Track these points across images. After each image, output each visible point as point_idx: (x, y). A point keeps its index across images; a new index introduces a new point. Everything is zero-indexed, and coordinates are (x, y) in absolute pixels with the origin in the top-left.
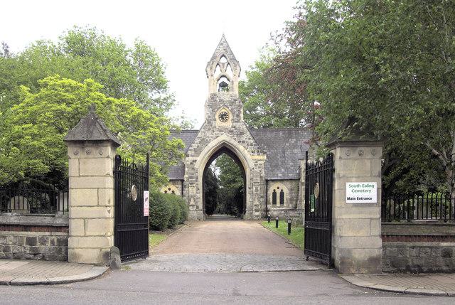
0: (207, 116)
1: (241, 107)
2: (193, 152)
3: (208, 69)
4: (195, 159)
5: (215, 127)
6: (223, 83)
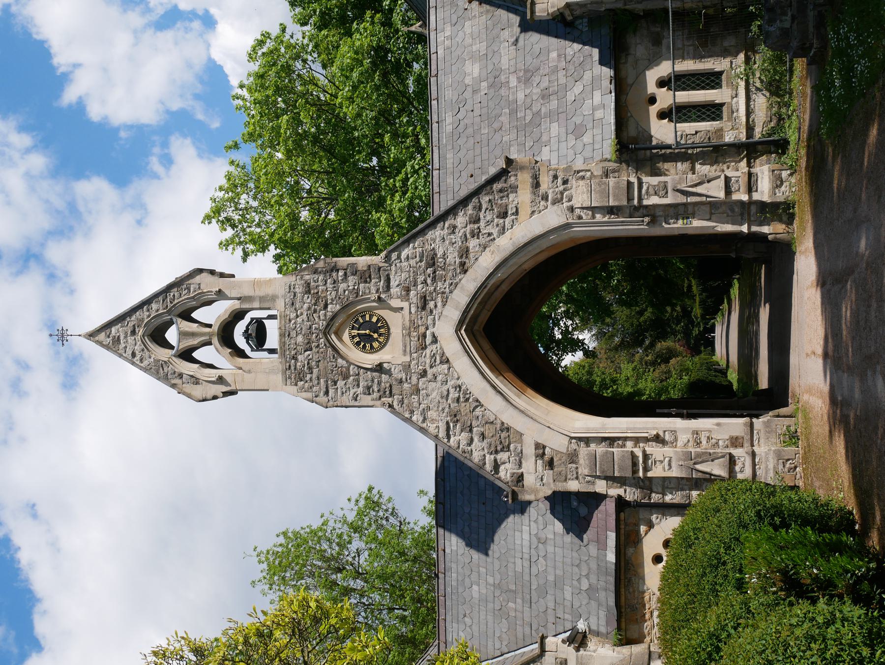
0: (367, 400)
1: (335, 269)
2: (502, 456)
3: (198, 391)
4: (529, 450)
5: (407, 367)
6: (247, 335)
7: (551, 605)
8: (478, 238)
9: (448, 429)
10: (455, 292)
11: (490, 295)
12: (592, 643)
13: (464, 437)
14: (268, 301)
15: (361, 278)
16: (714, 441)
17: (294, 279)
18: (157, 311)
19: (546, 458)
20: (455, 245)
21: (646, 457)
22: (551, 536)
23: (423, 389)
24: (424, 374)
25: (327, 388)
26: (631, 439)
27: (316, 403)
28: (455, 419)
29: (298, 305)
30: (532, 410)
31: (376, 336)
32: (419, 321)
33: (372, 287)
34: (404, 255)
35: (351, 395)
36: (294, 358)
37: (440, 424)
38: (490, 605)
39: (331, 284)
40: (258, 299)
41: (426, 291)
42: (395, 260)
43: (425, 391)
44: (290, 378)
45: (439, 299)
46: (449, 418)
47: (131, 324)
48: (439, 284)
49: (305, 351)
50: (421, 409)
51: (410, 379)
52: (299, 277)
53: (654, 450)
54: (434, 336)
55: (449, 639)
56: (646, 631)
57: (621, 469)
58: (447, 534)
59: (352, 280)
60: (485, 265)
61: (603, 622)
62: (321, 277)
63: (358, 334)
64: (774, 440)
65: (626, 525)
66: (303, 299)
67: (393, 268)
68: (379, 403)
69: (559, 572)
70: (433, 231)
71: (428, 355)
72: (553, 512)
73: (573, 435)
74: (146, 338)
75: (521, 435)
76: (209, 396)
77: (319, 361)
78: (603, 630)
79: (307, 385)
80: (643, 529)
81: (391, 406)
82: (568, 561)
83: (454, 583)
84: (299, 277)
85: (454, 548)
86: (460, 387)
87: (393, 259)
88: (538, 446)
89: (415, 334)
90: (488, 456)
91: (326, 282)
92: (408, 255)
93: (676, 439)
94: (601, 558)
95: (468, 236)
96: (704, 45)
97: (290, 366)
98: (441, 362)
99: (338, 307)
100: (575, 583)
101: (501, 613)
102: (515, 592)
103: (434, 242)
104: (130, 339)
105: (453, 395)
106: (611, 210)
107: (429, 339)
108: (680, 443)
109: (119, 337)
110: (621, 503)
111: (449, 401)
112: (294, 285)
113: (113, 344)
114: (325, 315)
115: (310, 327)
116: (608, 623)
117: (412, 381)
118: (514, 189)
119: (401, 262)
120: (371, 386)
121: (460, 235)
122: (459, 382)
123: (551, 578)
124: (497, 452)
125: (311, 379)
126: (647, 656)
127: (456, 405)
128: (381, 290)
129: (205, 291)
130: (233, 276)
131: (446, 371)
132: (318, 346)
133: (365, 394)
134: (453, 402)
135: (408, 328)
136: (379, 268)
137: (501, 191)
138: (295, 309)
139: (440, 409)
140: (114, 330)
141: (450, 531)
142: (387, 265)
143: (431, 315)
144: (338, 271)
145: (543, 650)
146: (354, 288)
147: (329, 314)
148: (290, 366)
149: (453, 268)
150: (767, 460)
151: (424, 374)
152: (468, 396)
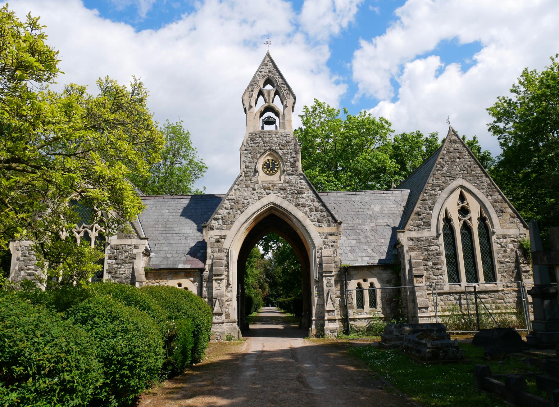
0: (243, 166)
1: (296, 153)
2: (221, 222)
3: (246, 98)
4: (223, 233)
5: (256, 182)
6: (269, 117)
7: (161, 242)
9: (232, 200)
10: (287, 202)
11: (287, 216)
12: (145, 259)
13: (229, 206)
16: (228, 307)
19: (220, 240)
21: (221, 280)
22: (188, 242)
24: (254, 190)
25: (248, 150)
26: (229, 274)
29: (281, 138)
30: (240, 233)
31: (269, 170)
34: (302, 181)
36: (260, 137)
37: (234, 196)
38: (160, 217)
44: (252, 135)
47: (273, 71)
48: (291, 196)
53: (224, 283)
54: (269, 193)
55: (146, 201)
56: (151, 280)
57: (216, 270)
58: (189, 200)
59: (292, 160)
60: (299, 214)
61: (154, 263)
62: (293, 147)
64: (228, 331)
65: (193, 272)
67: (297, 177)
68: (242, 171)
69: (174, 245)
72: (198, 242)
73: (230, 250)
75: (230, 229)
76: (244, 102)
78: (151, 263)
80: (192, 279)
81: (241, 176)
82: (179, 249)
83: (169, 202)
85: (183, 202)
88: (225, 236)
90: (221, 216)
93: (228, 292)
94: (180, 262)
96: (387, 301)
98: (259, 197)
99: (281, 154)
100: (170, 252)
101: (157, 222)
102: (166, 227)
104: (267, 70)
105: (246, 202)
106: (321, 265)
107: (268, 191)
108: (227, 293)
110: (202, 270)
111: (243, 200)
114: (277, 149)
115: (272, 143)
116: (154, 265)
118: (329, 225)
122: (251, 204)
123: (172, 242)
124: (222, 219)
125: (251, 143)
126: (140, 281)
130: (293, 112)
132: (265, 146)
136: (297, 171)
137: (328, 220)
140: (271, 63)
141: (190, 201)
144: (296, 154)
145: (142, 239)
147: (278, 151)
150: (221, 328)
151: (254, 190)
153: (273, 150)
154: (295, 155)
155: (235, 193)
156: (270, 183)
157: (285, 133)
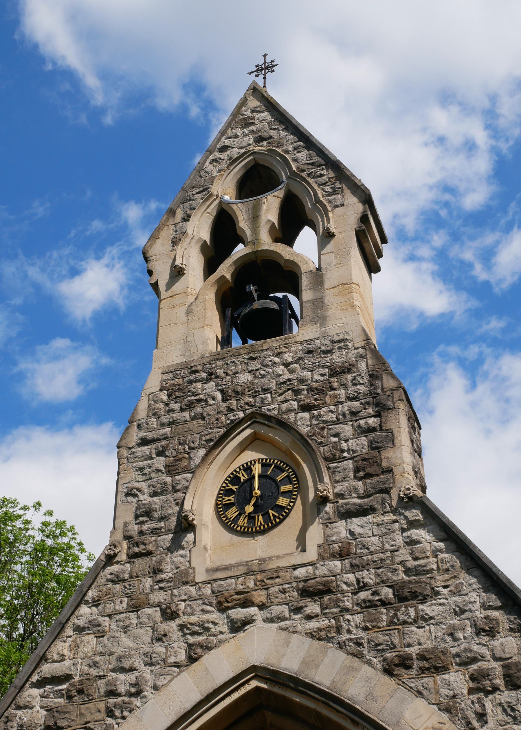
8: (471, 691)
9: (56, 680)
10: (342, 656)
14: (316, 312)
15: (364, 460)
17: (357, 345)
18: (295, 160)
20: (449, 639)
23: (138, 617)
27: (128, 428)
28: (74, 693)
31: (249, 509)
32: (276, 588)
33: (346, 484)
35: (137, 485)
36: (211, 375)
37: (67, 663)
39: (350, 408)
40: (319, 295)
41: (343, 592)
42: (406, 518)
43: (134, 621)
44: (174, 377)
45: (324, 622)
46: (77, 678)
47: (273, 133)
48: (358, 619)
49: (222, 391)
50: (100, 619)
51: (161, 588)
52: (362, 351)
54: (247, 622)
60: (408, 715)
63: (253, 477)
66: (319, 366)
67: (390, 517)
68: (119, 536)
70: (476, 586)
71: (206, 617)
74: (251, 157)
76: (152, 265)
77: (203, 418)
79: (162, 406)
84: (362, 351)
86: (138, 694)
87: (407, 513)
89: (251, 584)
91: (355, 399)
92: (418, 542)
95: (474, 667)
97: (196, 371)
99: (304, 430)
103: (453, 593)
109: (253, 124)
112: (347, 347)
113: (241, 120)
114: (289, 411)
115: (265, 391)
117: (156, 593)
119: (403, 530)
120: (151, 518)
121: (475, 648)
122: (148, 692)
125: (172, 411)
127: (103, 691)
128: (341, 501)
129: (330, 214)
131: (172, 660)
132: (230, 410)
133: (137, 508)
134: (108, 683)
135: (264, 567)
136: (386, 491)
138: (300, 358)
139: (97, 658)
140: (266, 115)
142: (394, 504)
143: (290, 611)
144: (378, 415)
146: (343, 451)
147: (292, 417)
148: (196, 371)
149: (396, 641)
152: (117, 713)
153: (269, 418)
154: (372, 422)
155: (76, 646)
156: (249, 572)
157: (324, 336)
